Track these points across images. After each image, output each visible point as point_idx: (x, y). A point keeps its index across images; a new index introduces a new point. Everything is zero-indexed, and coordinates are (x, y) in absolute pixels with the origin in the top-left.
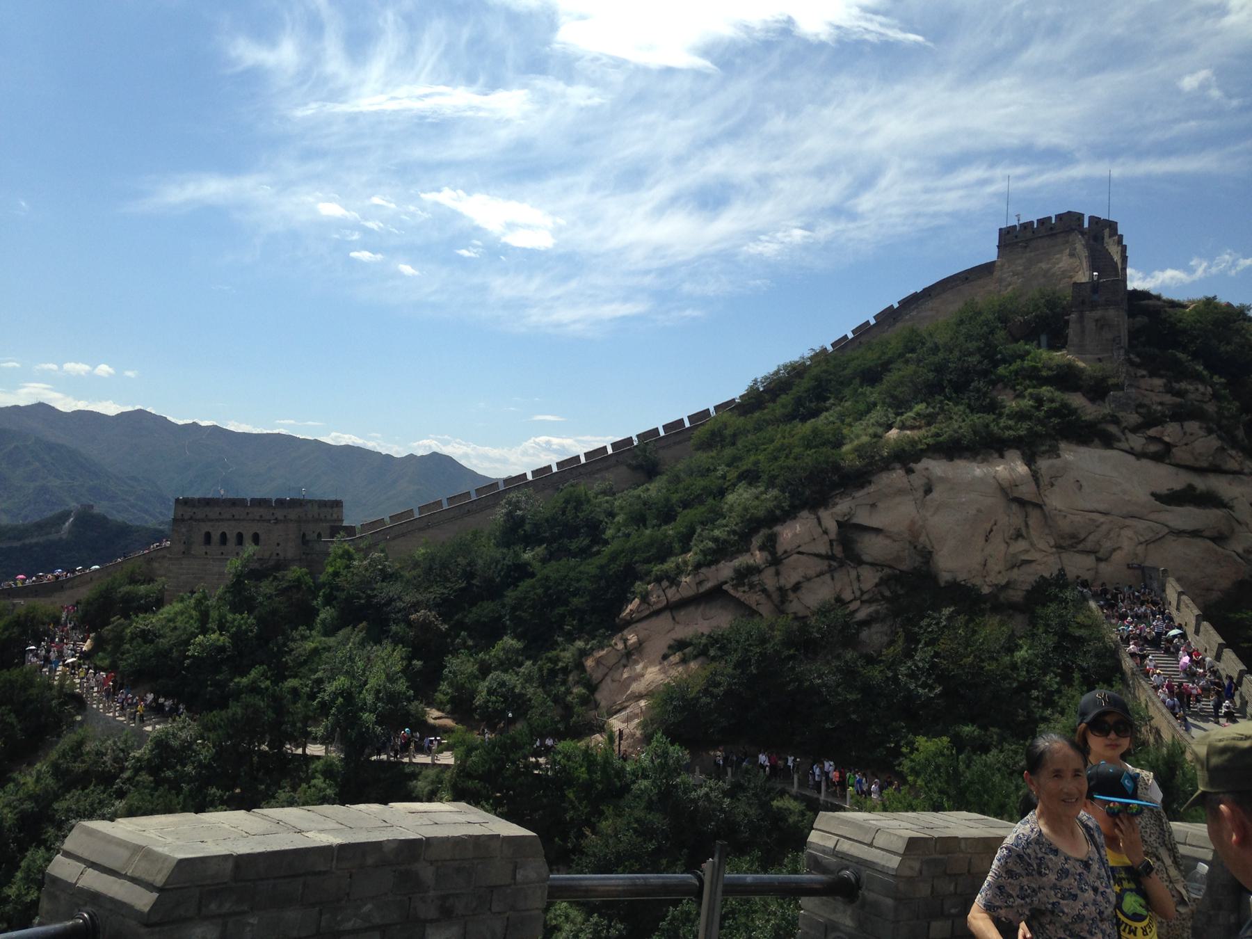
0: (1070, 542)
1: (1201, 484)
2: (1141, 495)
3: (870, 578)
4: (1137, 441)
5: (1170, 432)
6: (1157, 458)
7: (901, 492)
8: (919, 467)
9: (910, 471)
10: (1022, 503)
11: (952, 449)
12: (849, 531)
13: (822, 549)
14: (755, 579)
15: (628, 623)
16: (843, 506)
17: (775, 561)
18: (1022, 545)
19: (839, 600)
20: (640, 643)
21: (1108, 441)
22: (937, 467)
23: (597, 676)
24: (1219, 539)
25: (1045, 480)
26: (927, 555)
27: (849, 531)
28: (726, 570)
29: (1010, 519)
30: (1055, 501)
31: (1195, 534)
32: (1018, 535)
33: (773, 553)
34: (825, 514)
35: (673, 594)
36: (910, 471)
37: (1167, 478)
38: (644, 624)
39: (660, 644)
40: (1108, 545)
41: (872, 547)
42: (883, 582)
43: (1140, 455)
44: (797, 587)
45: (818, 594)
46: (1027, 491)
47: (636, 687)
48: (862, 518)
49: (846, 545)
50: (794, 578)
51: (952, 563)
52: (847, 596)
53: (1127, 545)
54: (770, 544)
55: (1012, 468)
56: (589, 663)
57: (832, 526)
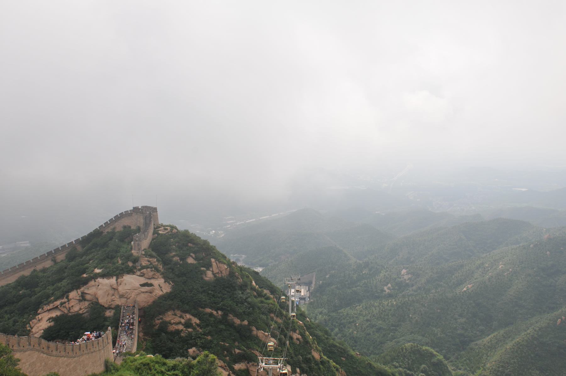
0: (122, 296)
1: (150, 282)
2: (137, 284)
3: (87, 303)
4: (138, 273)
5: (144, 271)
6: (142, 276)
7: (93, 286)
8: (97, 280)
9: (95, 281)
10: (114, 289)
11: (103, 276)
12: (83, 294)
13: (78, 298)
14: (64, 305)
15: (39, 314)
16: (82, 289)
17: (69, 301)
18: (114, 297)
19: (81, 309)
20: (42, 319)
21: (134, 273)
22: (100, 280)
23: (32, 325)
24: (151, 293)
25: (119, 284)
26: (97, 299)
27: (83, 294)
28: (58, 303)
29: (111, 292)
30: (120, 288)
31: (146, 292)
32: (113, 295)
33: (68, 299)
34: (78, 291)
35: (49, 308)
36: (95, 281)
37: (143, 280)
38: (44, 314)
39: (47, 318)
40: (129, 296)
41: (88, 297)
42: (89, 304)
43: (140, 276)
44: (72, 306)
45: (76, 309)
46: (115, 286)
47: (41, 328)
48: (86, 291)
49: (83, 298)
50: (72, 304)
51: (102, 301)
52: (82, 308)
53: (133, 296)
54: (67, 297)
55: (113, 280)
56: (31, 323)
57: (80, 293)
